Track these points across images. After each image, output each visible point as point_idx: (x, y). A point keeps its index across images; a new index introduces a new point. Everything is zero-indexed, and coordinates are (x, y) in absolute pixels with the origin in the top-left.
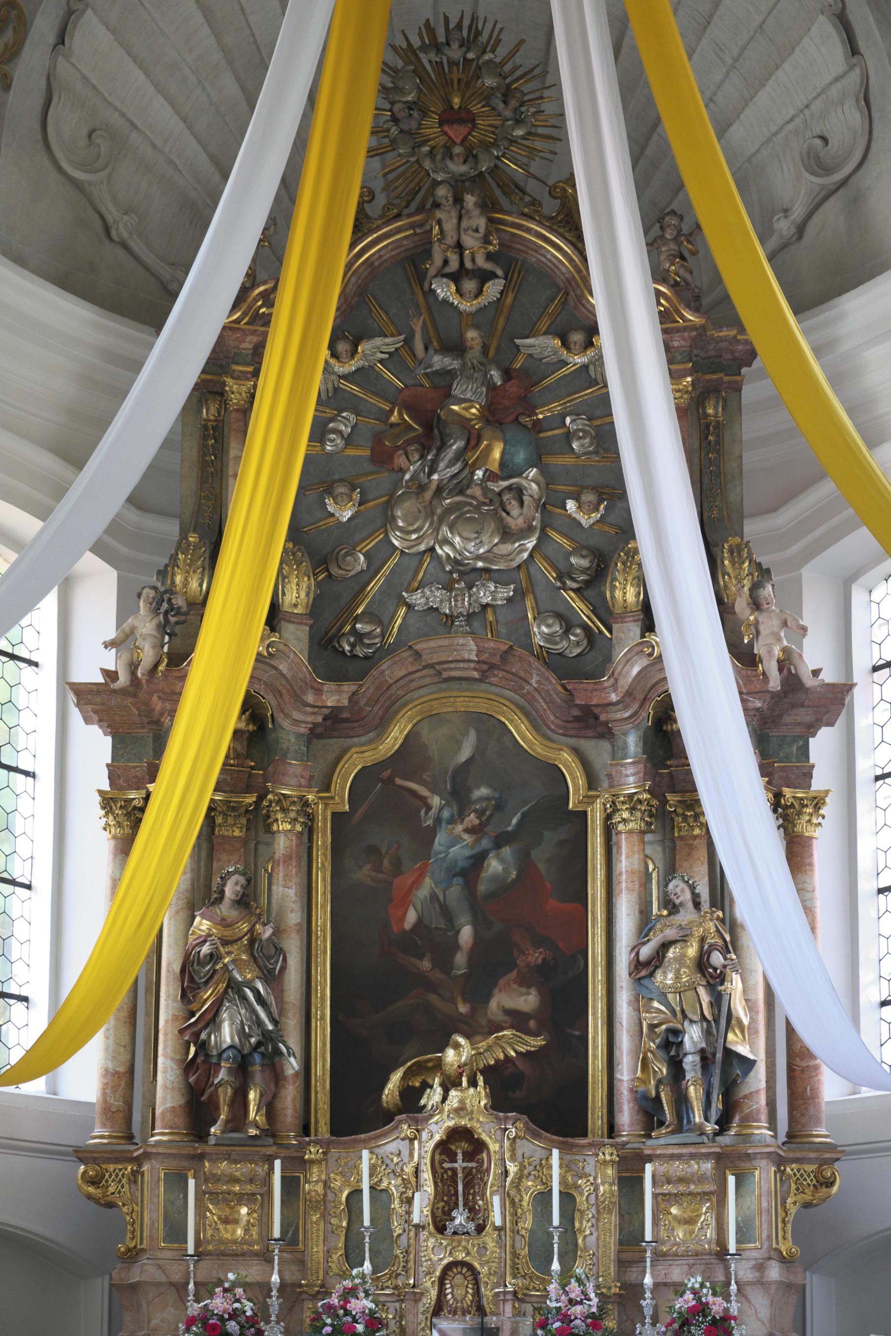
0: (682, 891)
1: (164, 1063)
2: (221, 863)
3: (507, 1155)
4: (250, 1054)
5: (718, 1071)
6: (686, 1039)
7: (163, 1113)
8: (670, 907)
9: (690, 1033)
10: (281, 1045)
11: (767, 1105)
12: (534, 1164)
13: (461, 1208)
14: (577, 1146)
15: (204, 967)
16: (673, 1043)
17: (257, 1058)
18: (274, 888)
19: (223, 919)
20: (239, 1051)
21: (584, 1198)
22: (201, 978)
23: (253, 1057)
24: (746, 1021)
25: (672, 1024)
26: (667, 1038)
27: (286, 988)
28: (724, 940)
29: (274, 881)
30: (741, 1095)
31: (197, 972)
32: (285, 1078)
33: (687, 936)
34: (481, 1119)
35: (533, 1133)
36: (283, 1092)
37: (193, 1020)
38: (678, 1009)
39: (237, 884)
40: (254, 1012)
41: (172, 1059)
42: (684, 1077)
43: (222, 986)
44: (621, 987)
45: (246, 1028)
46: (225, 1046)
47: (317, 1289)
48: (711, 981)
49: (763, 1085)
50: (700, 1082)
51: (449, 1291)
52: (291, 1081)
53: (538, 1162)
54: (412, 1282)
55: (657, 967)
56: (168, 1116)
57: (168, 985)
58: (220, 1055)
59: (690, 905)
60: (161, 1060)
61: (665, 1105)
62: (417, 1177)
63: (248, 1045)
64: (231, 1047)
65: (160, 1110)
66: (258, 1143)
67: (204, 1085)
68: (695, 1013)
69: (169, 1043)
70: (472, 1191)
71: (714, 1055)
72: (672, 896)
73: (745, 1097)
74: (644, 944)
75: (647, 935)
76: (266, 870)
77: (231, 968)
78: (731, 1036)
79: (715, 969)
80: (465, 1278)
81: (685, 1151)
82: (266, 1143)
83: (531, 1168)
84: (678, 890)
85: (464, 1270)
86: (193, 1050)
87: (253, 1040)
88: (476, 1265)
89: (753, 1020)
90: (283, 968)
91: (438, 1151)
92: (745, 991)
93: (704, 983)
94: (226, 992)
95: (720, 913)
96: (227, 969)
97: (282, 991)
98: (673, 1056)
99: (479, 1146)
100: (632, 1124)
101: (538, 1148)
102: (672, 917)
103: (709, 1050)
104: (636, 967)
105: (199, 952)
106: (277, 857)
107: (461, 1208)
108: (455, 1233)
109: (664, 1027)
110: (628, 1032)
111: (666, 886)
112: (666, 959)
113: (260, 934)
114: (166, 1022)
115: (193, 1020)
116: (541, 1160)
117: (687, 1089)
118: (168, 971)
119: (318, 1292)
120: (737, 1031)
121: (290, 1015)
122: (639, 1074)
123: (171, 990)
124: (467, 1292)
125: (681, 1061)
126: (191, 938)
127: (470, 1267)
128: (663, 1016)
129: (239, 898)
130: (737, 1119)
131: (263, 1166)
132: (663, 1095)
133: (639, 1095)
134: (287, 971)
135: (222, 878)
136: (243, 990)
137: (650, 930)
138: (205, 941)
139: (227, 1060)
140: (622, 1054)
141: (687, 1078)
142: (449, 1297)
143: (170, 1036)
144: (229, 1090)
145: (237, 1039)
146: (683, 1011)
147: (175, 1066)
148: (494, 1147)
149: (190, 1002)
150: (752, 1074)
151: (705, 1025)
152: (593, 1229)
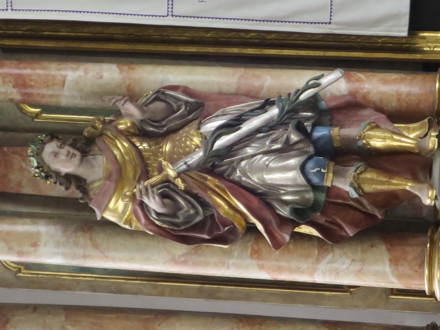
1: (324, 273)
2: (24, 183)
4: (315, 142)
7: (399, 277)
10: (303, 97)
15: (180, 208)
18: (64, 102)
19: (109, 177)
20: (309, 158)
22: (197, 213)
23: (319, 138)
27: (215, 89)
29: (53, 101)
31: (189, 219)
32: (352, 94)
36: (374, 97)
37: (260, 227)
39: (56, 154)
41: (318, 260)
43: (211, 181)
45: (277, 146)
46: (301, 180)
52: (357, 85)
56: (404, 269)
57: (206, 264)
58: (315, 188)
60: (319, 279)
63: (301, 145)
64: (303, 169)
65: (394, 280)
67: (358, 214)
69: (294, 264)
76: (37, 115)
77: (184, 167)
86: (305, 229)
87: (294, 138)
90: (186, 91)
94: (220, 176)
96: (184, 172)
97: (221, 93)
105: (158, 214)
106: (18, 97)
113: (133, 124)
114: (261, 267)
115: (260, 227)
118: (185, 263)
121: (257, 83)
123: (214, 259)
126: (136, 225)
129: (78, 154)
134: (191, 86)
135: (47, 177)
136: (217, 150)
138: (142, 205)
139: (322, 176)
143: (283, 264)
144: (368, 175)
145: (293, 162)
147: (329, 257)
149: (233, 231)
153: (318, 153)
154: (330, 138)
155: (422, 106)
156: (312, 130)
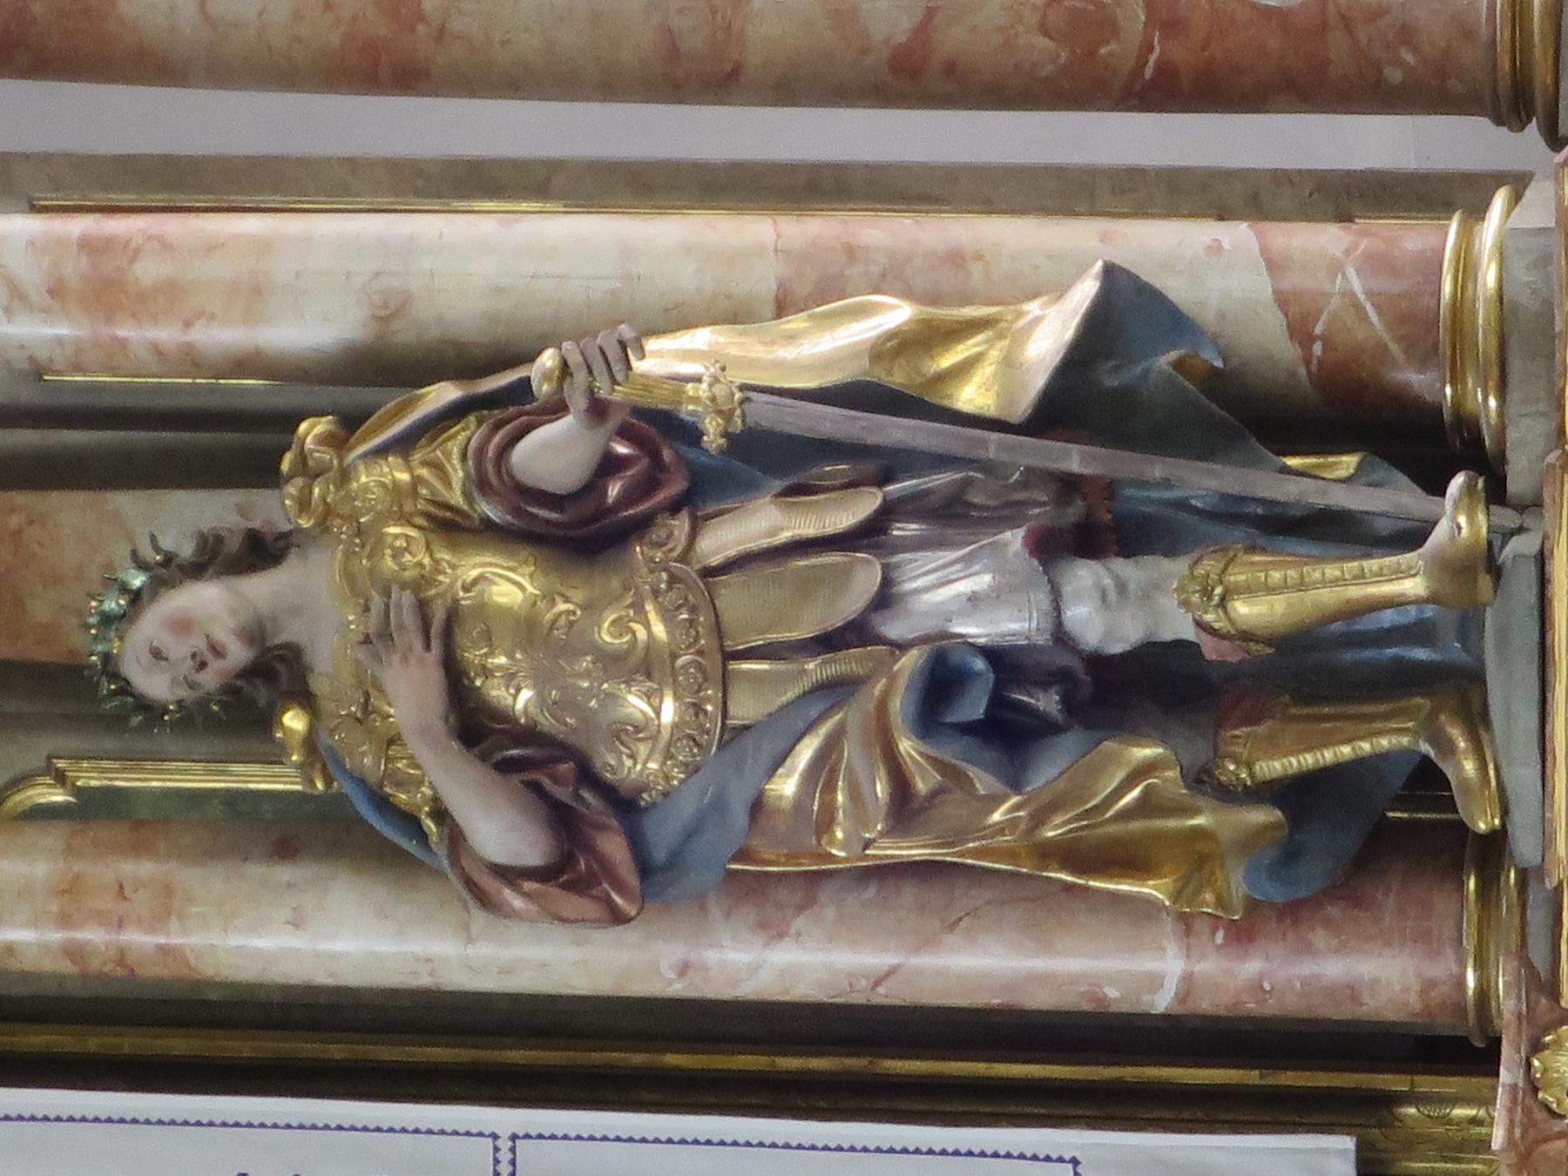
0: (182, 625)
5: (1157, 468)
6: (975, 629)
8: (262, 695)
11: (1345, 217)
16: (998, 701)
24: (897, 314)
26: (969, 729)
28: (455, 412)
30: (1286, 351)
33: (423, 607)
42: (1180, 645)
44: (684, 969)
48: (675, 487)
49: (1237, 235)
55: (587, 775)
59: (261, 588)
61: (1328, 756)
71: (1069, 485)
72: (210, 680)
73: (1300, 331)
74: (456, 838)
75: (410, 822)
78: (972, 396)
79: (609, 465)
84: (179, 649)
89: (892, 279)
92: (734, 314)
93: (680, 525)
95: (312, 430)
102: (319, 685)
103: (1042, 513)
104: (580, 886)
109: (907, 746)
110: (927, 942)
111: (150, 710)
112: (546, 722)
120: (947, 361)
122: (1152, 889)
125: (1098, 663)
128: (851, 751)
130: (1416, 379)
132: (1274, 767)
133: (1275, 893)
137: (383, 804)
140: (1044, 979)
146: (827, 643)
150: (1176, 289)
151: (905, 530)
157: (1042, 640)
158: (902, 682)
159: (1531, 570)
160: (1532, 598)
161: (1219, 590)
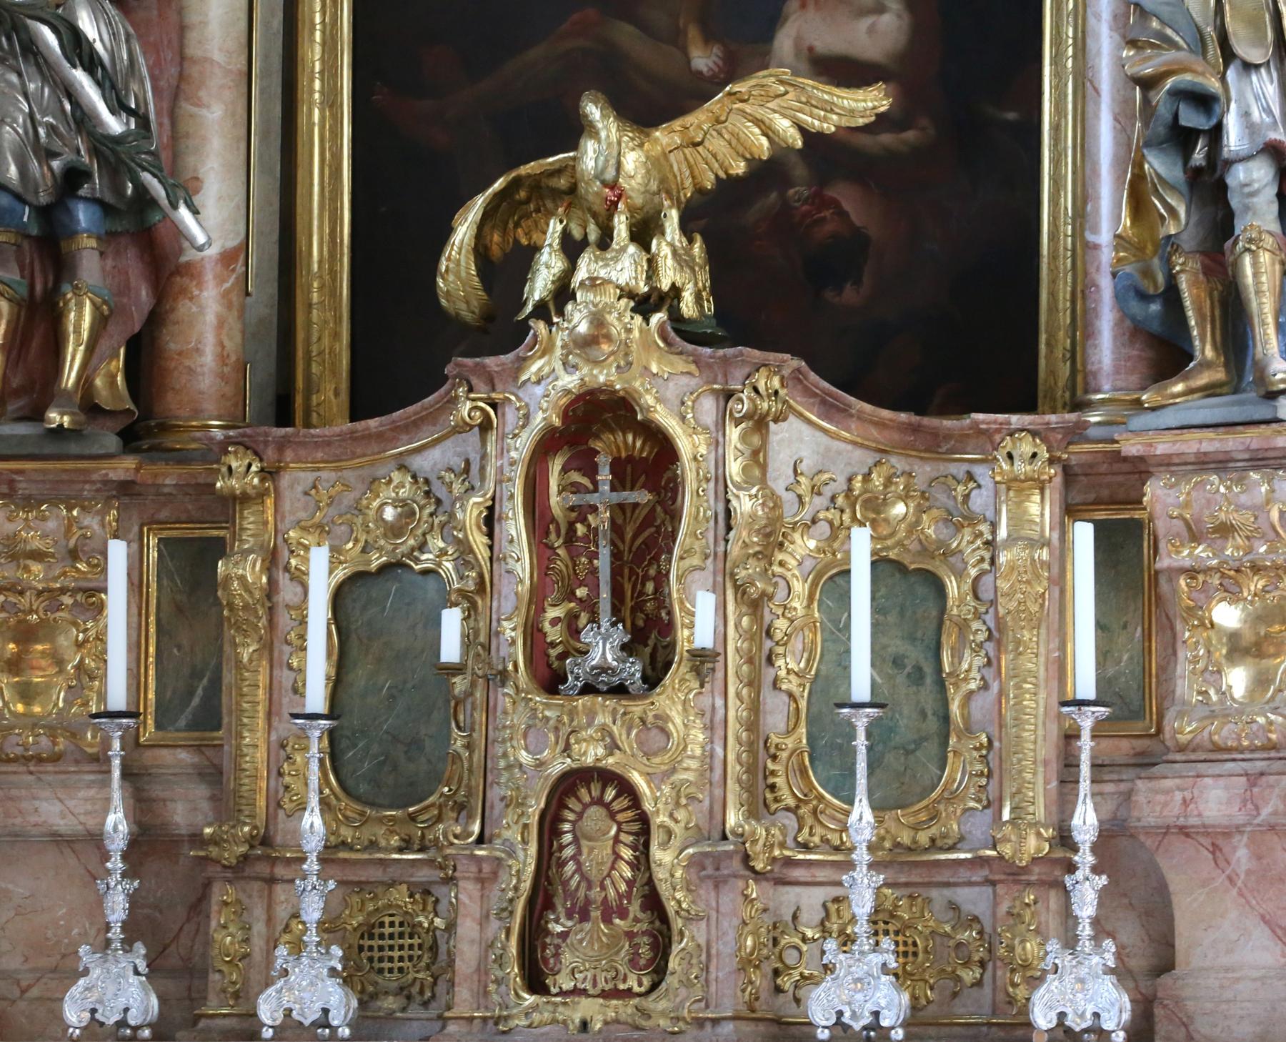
3: (734, 468)
9: (1241, 99)
12: (828, 491)
13: (605, 622)
14: (948, 436)
17: (83, 215)
21: (967, 586)
23: (71, 214)
25: (1188, 77)
27: (192, 18)
32: (189, 271)
34: (654, 369)
35: (824, 402)
36: (184, 308)
38: (1209, 30)
40: (70, 92)
47: (243, 849)
50: (1269, 241)
51: (568, 852)
53: (841, 485)
54: (476, 828)
61: (1190, 313)
62: (490, 535)
66: (74, 448)
68: (1259, 41)
70: (652, 572)
80: (612, 815)
81: (1233, 442)
82: (96, 450)
83: (818, 501)
85: (610, 794)
88: (638, 779)
91: (556, 466)
97: (182, 29)
98: (1198, 171)
99: (665, 450)
100: (1117, 370)
101: (842, 446)
107: (605, 622)
108: (588, 689)
116: (850, 480)
117: (1237, 265)
119: (245, 858)
124: (618, 857)
127: (627, 789)
131: (103, 513)
132: (1184, 283)
141: (1237, 232)
142: (570, 867)
148: (687, 444)
152: (989, 673)
153: (44, 213)
154: (73, 234)
155: (170, 396)
156: (86, 199)
157: (1225, 153)
158: (1199, 79)
159: (1269, 416)
160: (1257, 417)
161: (1253, 247)
